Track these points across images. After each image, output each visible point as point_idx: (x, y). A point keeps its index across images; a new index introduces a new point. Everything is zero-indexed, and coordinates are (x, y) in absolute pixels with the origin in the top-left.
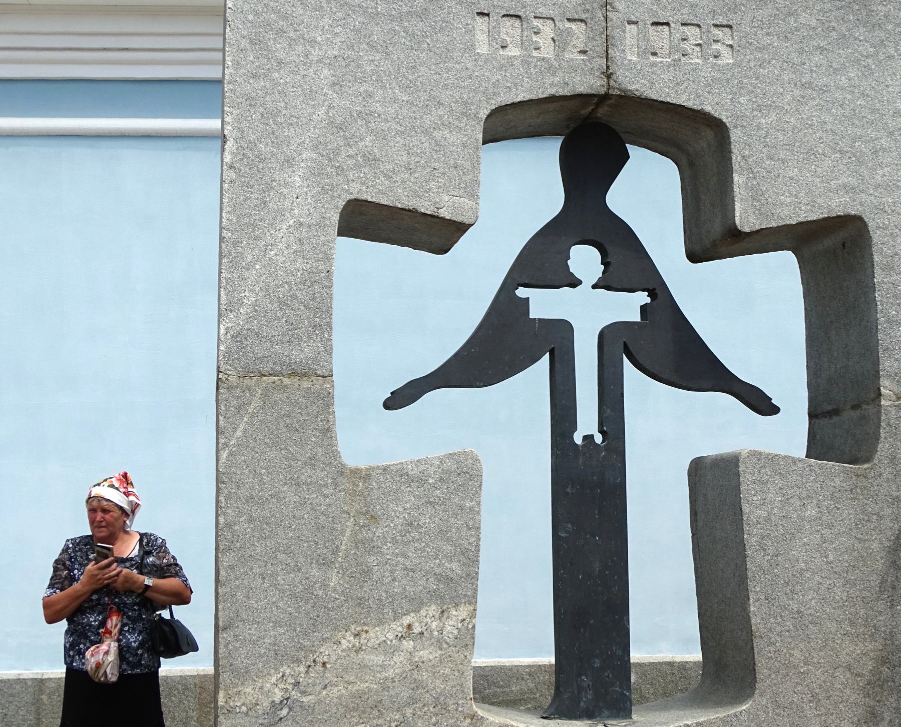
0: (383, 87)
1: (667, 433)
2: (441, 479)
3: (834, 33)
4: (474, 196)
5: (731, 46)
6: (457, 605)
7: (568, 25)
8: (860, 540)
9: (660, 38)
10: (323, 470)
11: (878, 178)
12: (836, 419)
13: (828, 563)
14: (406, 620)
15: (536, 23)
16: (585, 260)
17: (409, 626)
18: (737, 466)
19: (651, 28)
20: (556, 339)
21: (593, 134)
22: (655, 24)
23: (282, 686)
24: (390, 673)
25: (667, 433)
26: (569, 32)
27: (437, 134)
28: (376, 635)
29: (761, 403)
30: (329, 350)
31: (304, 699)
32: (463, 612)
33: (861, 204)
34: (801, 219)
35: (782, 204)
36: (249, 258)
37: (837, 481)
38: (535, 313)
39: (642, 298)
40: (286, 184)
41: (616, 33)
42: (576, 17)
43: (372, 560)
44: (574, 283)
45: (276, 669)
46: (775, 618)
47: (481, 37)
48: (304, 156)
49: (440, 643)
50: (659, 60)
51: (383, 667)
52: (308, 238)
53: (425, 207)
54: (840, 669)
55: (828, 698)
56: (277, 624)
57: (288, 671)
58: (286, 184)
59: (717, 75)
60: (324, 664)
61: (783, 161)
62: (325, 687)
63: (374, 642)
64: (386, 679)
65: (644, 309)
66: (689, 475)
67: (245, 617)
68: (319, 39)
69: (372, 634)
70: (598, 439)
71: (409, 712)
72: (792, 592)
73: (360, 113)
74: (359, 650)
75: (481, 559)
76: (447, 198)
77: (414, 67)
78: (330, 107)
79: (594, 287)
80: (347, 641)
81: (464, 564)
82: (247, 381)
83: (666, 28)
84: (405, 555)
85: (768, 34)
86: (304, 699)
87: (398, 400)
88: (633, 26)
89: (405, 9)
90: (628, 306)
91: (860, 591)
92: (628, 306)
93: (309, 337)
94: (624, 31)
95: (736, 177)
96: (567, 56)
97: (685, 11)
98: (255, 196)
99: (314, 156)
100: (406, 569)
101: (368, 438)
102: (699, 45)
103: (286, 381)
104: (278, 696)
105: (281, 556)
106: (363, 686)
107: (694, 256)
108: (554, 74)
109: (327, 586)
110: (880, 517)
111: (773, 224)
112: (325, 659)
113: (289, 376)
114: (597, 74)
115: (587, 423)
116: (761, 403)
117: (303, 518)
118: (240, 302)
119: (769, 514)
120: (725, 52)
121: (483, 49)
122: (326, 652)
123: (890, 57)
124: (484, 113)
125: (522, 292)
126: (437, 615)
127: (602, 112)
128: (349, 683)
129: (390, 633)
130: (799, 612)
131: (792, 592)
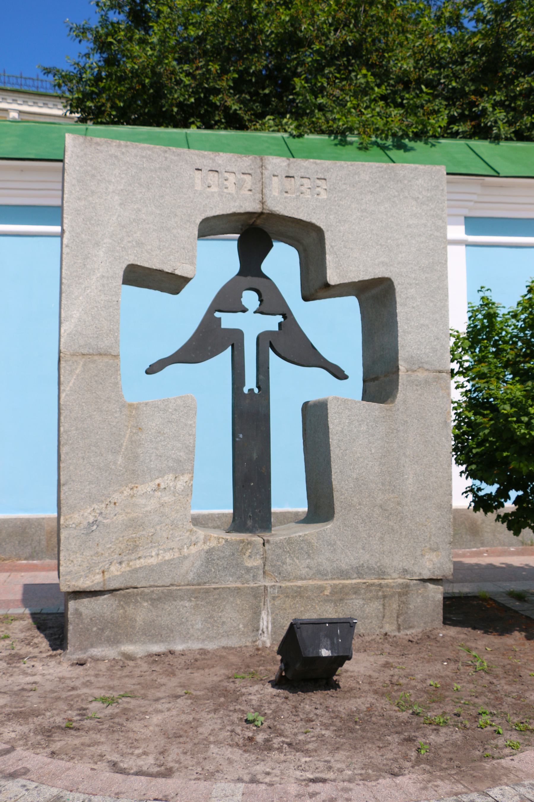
1: (291, 387)
2: (175, 410)
3: (378, 185)
4: (192, 263)
5: (326, 189)
6: (183, 474)
7: (243, 176)
8: (388, 443)
10: (114, 404)
11: (399, 259)
12: (376, 382)
13: (371, 454)
14: (157, 481)
15: (227, 175)
16: (250, 299)
17: (159, 485)
18: (327, 405)
20: (234, 340)
21: (255, 234)
22: (287, 177)
23: (93, 514)
24: (149, 508)
25: (291, 387)
26: (244, 181)
27: (175, 231)
29: (339, 374)
30: (117, 342)
31: (105, 521)
32: (186, 477)
33: (391, 272)
35: (351, 271)
37: (377, 412)
40: (96, 256)
42: (247, 172)
43: (139, 450)
44: (244, 310)
47: (198, 182)
48: (105, 241)
50: (289, 195)
51: (145, 505)
52: (107, 284)
53: (168, 269)
56: (91, 483)
58: (96, 256)
59: (318, 204)
60: (115, 503)
61: (352, 249)
62: (115, 515)
64: (147, 511)
65: (280, 324)
66: (302, 410)
67: (74, 479)
68: (113, 180)
69: (139, 488)
71: (158, 528)
73: (134, 220)
74: (132, 496)
75: (196, 451)
77: (162, 196)
78: (119, 216)
79: (255, 312)
81: (187, 453)
82: (75, 358)
83: (292, 179)
84: (157, 449)
85: (344, 184)
86: (105, 521)
87: (153, 369)
88: (276, 178)
89: (158, 166)
90: (272, 323)
91: (387, 468)
92: (272, 323)
93: (107, 335)
94: (271, 180)
95: (327, 257)
96: (242, 192)
97: (302, 170)
100: (157, 455)
101: (137, 388)
102: (309, 188)
103: (96, 358)
105: (93, 448)
106: (135, 515)
107: (306, 298)
108: (235, 201)
109: (117, 464)
111: (346, 281)
112: (116, 501)
114: (257, 201)
115: (250, 382)
116: (339, 374)
117: (104, 428)
118: (72, 317)
119: (343, 429)
120: (323, 193)
121: (199, 187)
123: (406, 197)
124: (198, 221)
125: (217, 314)
126: (173, 479)
127: (258, 222)
128: (128, 513)
129: (148, 487)
131: (353, 468)
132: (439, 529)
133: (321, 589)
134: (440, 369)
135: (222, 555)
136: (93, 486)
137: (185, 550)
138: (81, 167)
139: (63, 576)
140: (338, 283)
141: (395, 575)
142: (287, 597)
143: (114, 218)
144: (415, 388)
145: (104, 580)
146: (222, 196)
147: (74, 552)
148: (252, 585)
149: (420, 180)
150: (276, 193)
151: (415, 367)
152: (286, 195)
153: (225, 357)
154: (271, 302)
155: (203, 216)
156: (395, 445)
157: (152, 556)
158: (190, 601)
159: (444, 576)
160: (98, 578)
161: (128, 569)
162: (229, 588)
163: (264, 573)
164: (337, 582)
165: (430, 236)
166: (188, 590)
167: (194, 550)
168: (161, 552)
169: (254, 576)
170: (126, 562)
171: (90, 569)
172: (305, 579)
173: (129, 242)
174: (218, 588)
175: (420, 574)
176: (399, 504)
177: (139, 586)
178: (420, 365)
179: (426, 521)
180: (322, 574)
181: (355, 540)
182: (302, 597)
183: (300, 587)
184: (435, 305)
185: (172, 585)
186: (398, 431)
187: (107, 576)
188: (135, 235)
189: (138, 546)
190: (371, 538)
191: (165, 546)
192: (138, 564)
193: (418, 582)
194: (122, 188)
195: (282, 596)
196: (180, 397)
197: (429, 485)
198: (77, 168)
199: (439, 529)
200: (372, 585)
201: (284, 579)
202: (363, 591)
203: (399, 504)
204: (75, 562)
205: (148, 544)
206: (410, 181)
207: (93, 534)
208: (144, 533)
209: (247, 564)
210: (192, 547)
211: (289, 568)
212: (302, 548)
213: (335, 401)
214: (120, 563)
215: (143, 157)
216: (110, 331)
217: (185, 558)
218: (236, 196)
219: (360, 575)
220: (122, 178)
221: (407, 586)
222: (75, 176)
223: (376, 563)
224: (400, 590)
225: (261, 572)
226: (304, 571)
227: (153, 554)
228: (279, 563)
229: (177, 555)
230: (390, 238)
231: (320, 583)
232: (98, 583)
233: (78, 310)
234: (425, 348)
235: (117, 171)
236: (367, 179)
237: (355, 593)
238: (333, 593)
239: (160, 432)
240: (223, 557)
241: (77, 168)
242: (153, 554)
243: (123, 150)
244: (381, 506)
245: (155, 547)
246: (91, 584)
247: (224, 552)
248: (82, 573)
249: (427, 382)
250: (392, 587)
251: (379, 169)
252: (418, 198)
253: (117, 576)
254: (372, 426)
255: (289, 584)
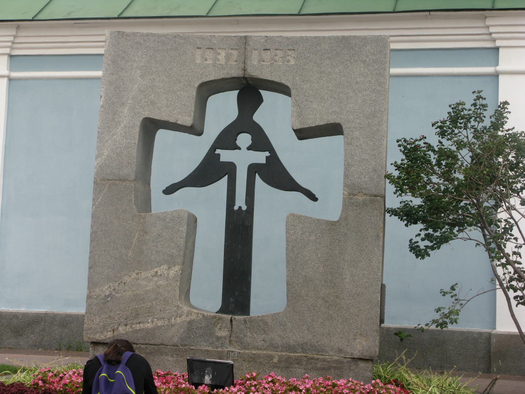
0: (159, 76)
3: (335, 52)
6: (174, 266)
7: (231, 51)
9: (267, 56)
14: (156, 270)
15: (220, 51)
16: (244, 139)
17: (157, 272)
19: (263, 51)
20: (230, 169)
24: (148, 288)
26: (231, 54)
27: (179, 93)
28: (144, 275)
32: (177, 268)
33: (341, 119)
34: (317, 124)
36: (107, 138)
38: (222, 159)
39: (267, 154)
40: (122, 112)
41: (249, 54)
44: (239, 148)
45: (108, 284)
46: (296, 278)
49: (167, 279)
54: (320, 299)
55: (314, 310)
57: (112, 285)
58: (122, 112)
60: (125, 283)
62: (125, 291)
63: (143, 277)
64: (147, 290)
69: (143, 274)
70: (244, 208)
71: (154, 303)
72: (303, 268)
74: (137, 279)
76: (180, 117)
80: (134, 275)
82: (103, 182)
84: (157, 246)
85: (309, 53)
89: (169, 47)
90: (261, 157)
92: (261, 157)
94: (252, 53)
97: (277, 44)
98: (110, 116)
99: (132, 102)
100: (156, 251)
102: (281, 57)
103: (117, 182)
104: (108, 293)
105: (112, 244)
110: (339, 241)
111: (306, 126)
113: (118, 180)
115: (240, 202)
116: (313, 197)
118: (103, 154)
122: (126, 279)
124: (197, 85)
125: (218, 151)
126: (167, 268)
128: (133, 291)
129: (149, 274)
130: (305, 276)
131: (303, 268)
132: (369, 319)
133: (271, 357)
134: (376, 193)
135: (199, 326)
136: (110, 270)
137: (173, 320)
138: (115, 52)
139: (86, 330)
140: (299, 128)
141: (331, 353)
142: (244, 361)
143: (136, 86)
144: (355, 208)
145: (114, 336)
146: (215, 66)
147: (94, 315)
148: (220, 349)
149: (368, 47)
150: (255, 63)
151: (355, 192)
152: (262, 63)
153: (224, 181)
154: (260, 142)
155: (200, 82)
156: (337, 252)
157: (148, 323)
158: (173, 356)
159: (370, 357)
160: (110, 334)
161: (131, 330)
162: (201, 350)
163: (230, 341)
164: (284, 354)
165: (374, 90)
166: (172, 349)
167: (179, 320)
168: (155, 320)
169: (222, 344)
170: (130, 325)
171: (105, 327)
172: (261, 349)
173: (145, 102)
174: (193, 349)
175: (352, 354)
176: (337, 297)
177: (137, 343)
178: (360, 191)
179: (358, 312)
180: (274, 347)
181: (302, 323)
182: (255, 362)
183: (254, 354)
184: (375, 144)
185: (162, 344)
186: (339, 241)
187: (116, 333)
188: (150, 97)
189: (139, 314)
190: (314, 323)
191: (158, 316)
192: (138, 327)
193: (350, 359)
194: (143, 64)
195: (240, 360)
196: (175, 211)
197: (362, 284)
198: (112, 53)
199: (369, 319)
200: (313, 358)
201: (245, 348)
202: (304, 363)
203: (337, 297)
204: (95, 322)
205: (146, 313)
206: (360, 48)
207: (108, 303)
208: (144, 305)
209: (217, 334)
210: (178, 319)
211: (249, 340)
212: (260, 326)
213: (292, 217)
214: (126, 325)
215: (159, 42)
216: (129, 164)
217: (173, 325)
218: (225, 66)
219: (304, 350)
220: (143, 58)
221: (342, 362)
222: (110, 59)
223: (317, 342)
224: (335, 365)
225: (227, 341)
226: (260, 343)
227: (150, 321)
228: (242, 336)
229: (166, 323)
230: (342, 92)
231: (270, 353)
232: (109, 338)
233: (107, 150)
234: (365, 177)
235: (140, 53)
236: (327, 48)
237: (298, 363)
238: (280, 361)
239: (159, 235)
240: (200, 328)
241: (112, 53)
242: (150, 321)
243: (145, 38)
244: (323, 298)
245: (151, 316)
246: (104, 338)
247: (201, 324)
248: (99, 330)
249: (364, 204)
250: (329, 362)
251: (337, 40)
252: (366, 61)
253: (123, 334)
254: (319, 236)
255: (247, 351)
